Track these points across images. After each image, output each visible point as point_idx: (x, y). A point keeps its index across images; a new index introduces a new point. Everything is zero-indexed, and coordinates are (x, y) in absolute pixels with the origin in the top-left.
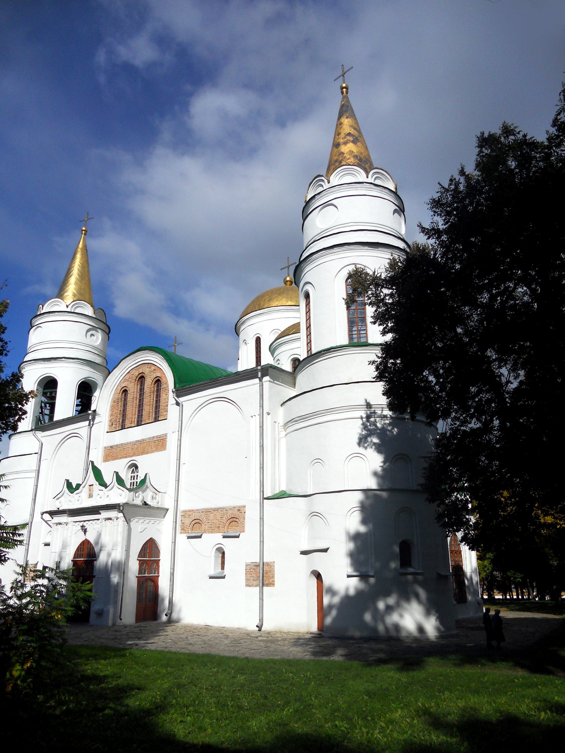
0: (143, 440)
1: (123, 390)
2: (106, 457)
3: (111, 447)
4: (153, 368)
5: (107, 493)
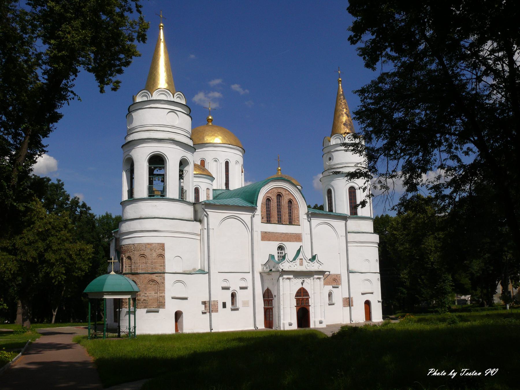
1: (269, 198)
3: (266, 232)
4: (287, 192)
5: (313, 265)
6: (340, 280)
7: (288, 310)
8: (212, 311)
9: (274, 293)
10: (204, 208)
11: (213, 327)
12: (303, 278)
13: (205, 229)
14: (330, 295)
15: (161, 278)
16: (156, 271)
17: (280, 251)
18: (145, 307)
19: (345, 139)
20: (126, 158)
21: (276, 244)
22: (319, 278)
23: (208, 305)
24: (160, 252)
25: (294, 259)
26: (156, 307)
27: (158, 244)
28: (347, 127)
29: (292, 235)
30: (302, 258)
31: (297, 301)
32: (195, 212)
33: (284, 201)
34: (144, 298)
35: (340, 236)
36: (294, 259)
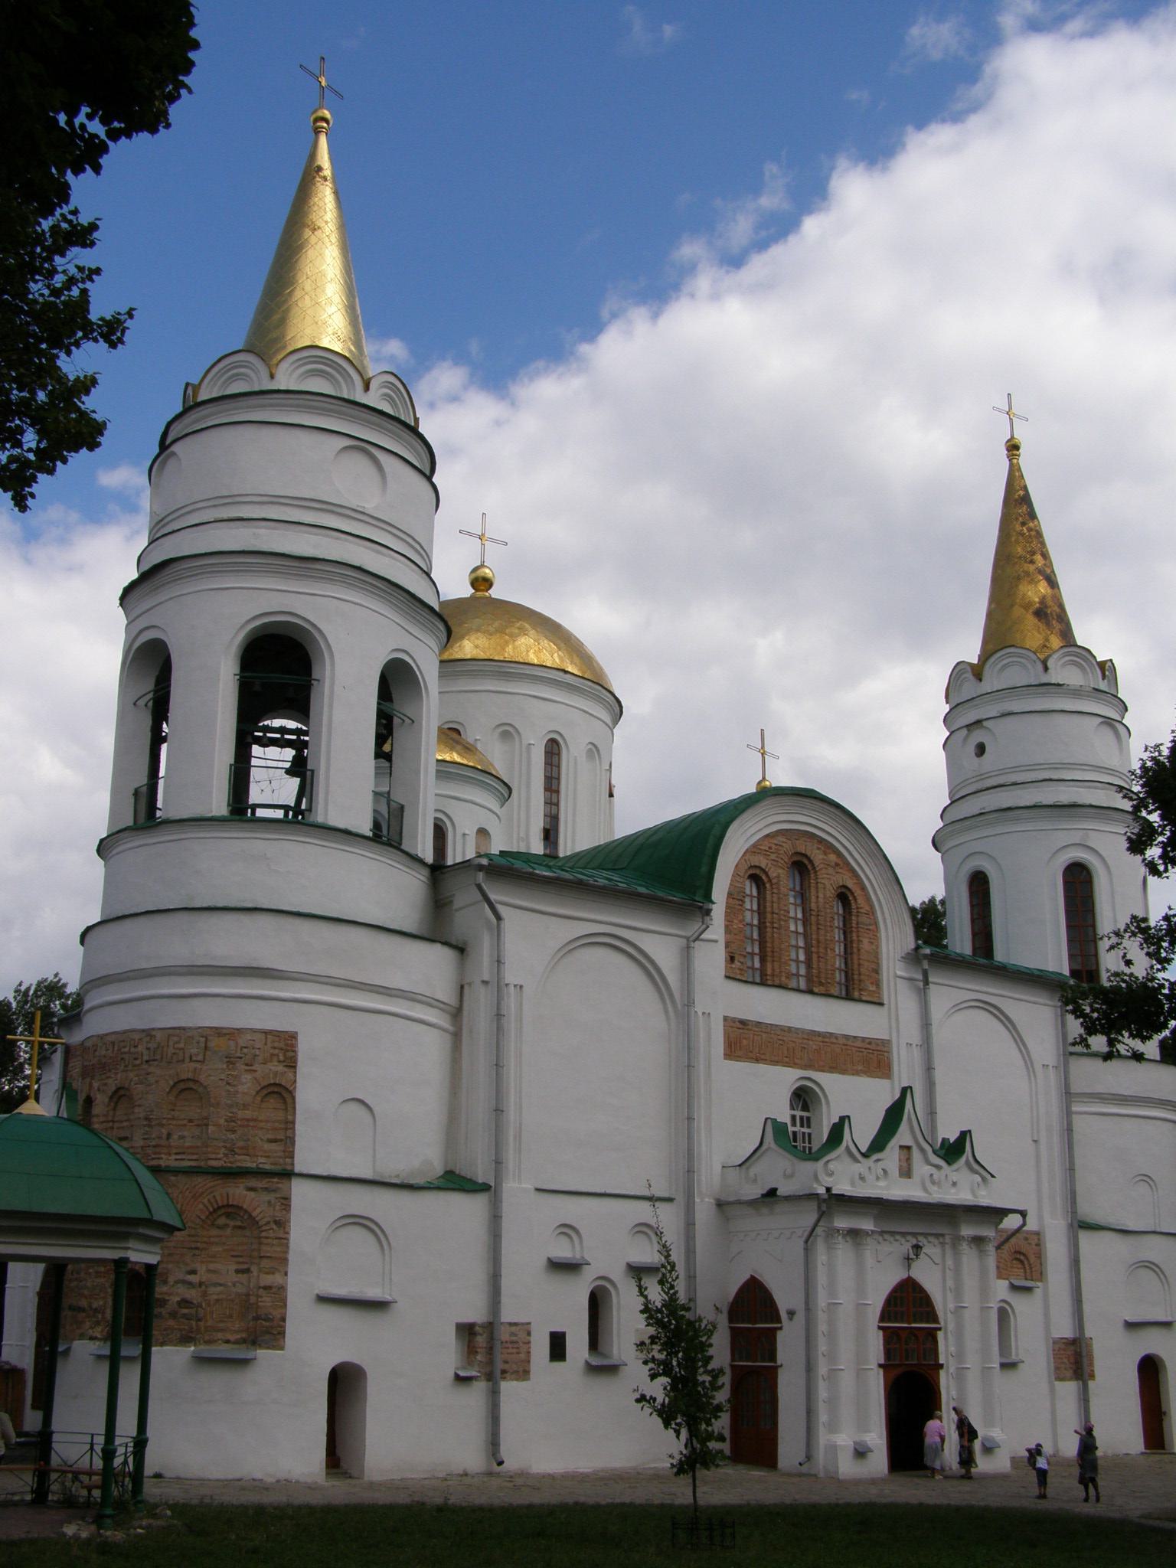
0: (831, 1034)
1: (758, 872)
2: (730, 1045)
3: (743, 1022)
4: (833, 857)
5: (954, 1177)
6: (1040, 1255)
7: (847, 1381)
8: (504, 1372)
9: (785, 1298)
10: (483, 885)
11: (504, 1452)
12: (914, 1235)
13: (485, 983)
14: (1003, 1315)
15: (271, 1197)
16: (249, 1164)
17: (798, 1113)
18: (186, 1340)
19: (1046, 669)
20: (137, 645)
21: (788, 1078)
22: (978, 1241)
23: (481, 1340)
24: (276, 1074)
25: (878, 1144)
26: (236, 1342)
27: (266, 1033)
28: (1048, 625)
29: (850, 1043)
30: (908, 1141)
31: (887, 1341)
32: (439, 904)
33: (821, 895)
34: (184, 1292)
35: (1038, 1067)
36: (878, 1144)
